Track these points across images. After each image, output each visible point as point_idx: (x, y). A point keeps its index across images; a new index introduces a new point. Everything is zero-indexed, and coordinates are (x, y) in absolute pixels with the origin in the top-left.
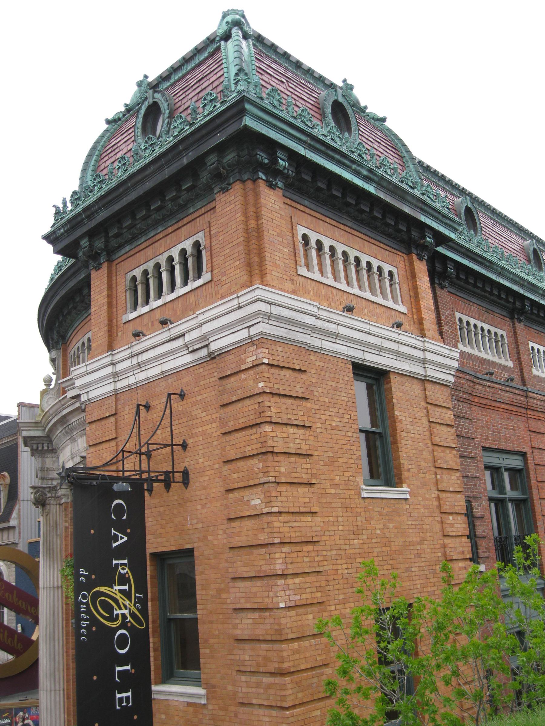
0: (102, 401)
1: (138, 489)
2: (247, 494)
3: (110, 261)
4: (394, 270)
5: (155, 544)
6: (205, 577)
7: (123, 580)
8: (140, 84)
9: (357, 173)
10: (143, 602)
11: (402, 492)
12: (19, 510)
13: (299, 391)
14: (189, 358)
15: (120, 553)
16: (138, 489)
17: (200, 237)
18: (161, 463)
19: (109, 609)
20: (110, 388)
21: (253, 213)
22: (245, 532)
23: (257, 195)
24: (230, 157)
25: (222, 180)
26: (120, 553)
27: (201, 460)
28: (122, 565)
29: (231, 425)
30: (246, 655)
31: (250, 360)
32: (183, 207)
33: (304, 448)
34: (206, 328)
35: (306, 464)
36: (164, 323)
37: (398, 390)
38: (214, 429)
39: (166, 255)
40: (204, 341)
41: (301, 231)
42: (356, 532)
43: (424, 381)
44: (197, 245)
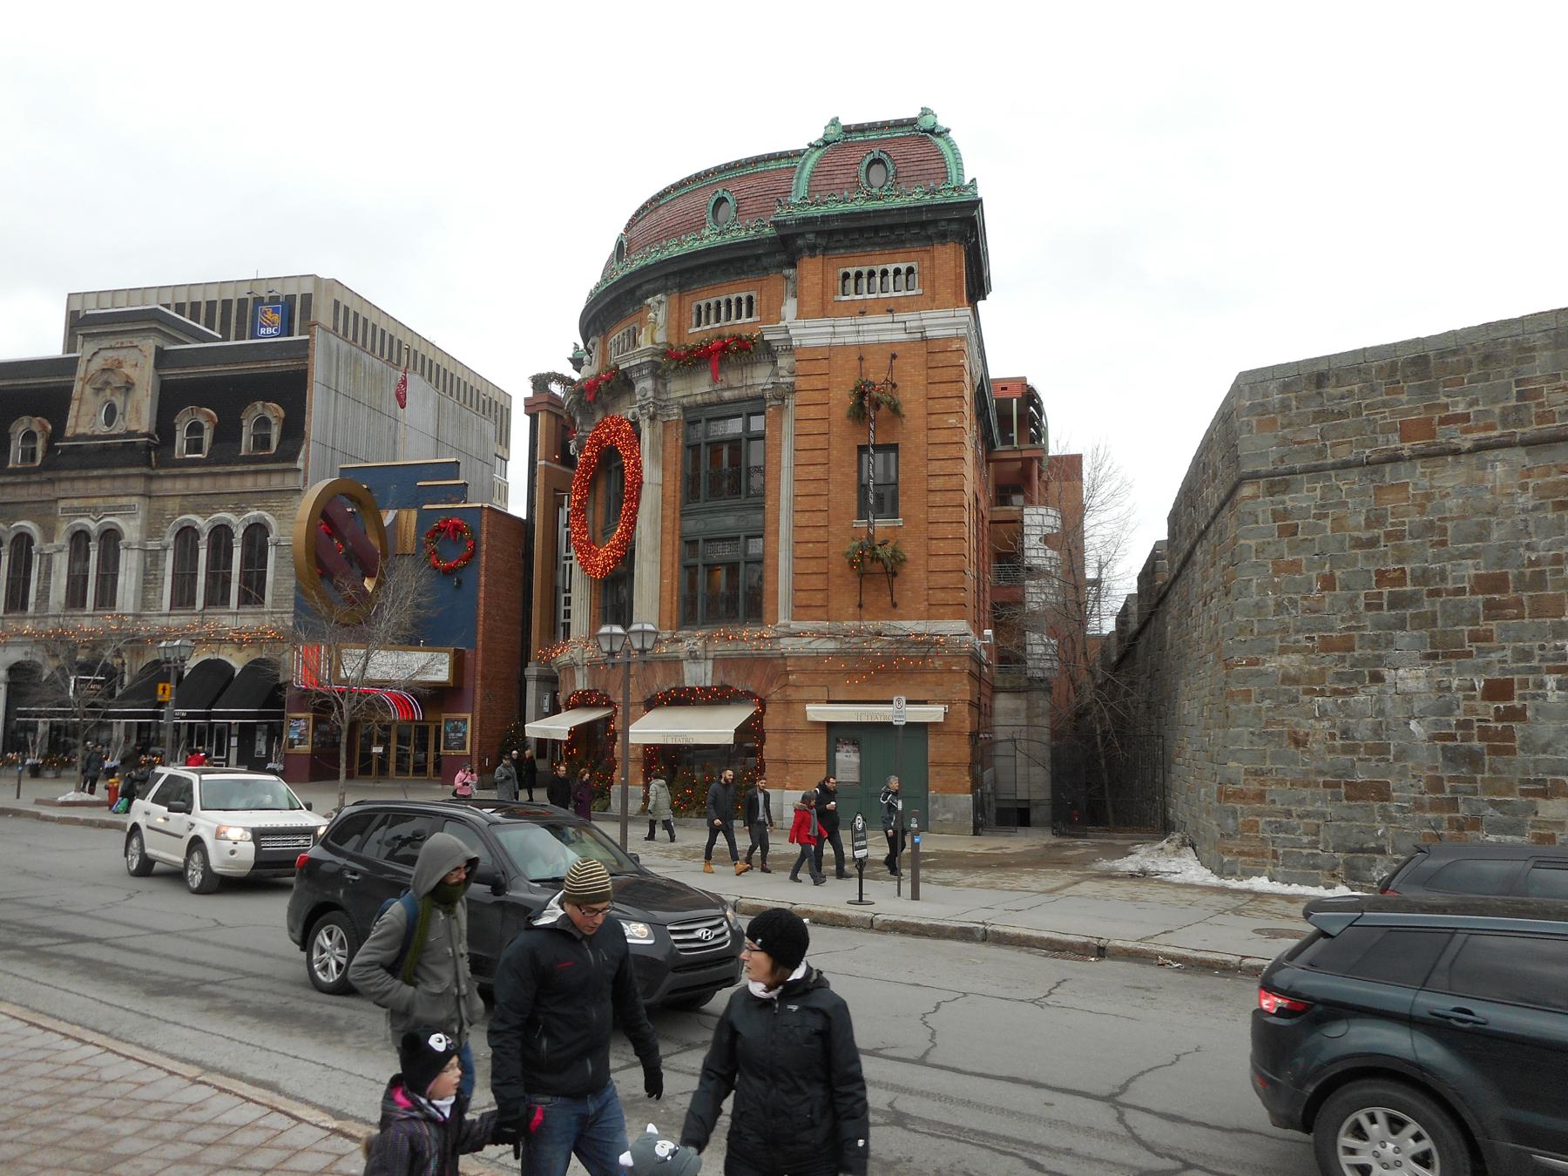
2: (945, 417)
12: (307, 452)
14: (905, 336)
17: (914, 265)
20: (825, 341)
22: (942, 436)
24: (954, 227)
25: (943, 237)
29: (937, 379)
30: (938, 499)
31: (954, 347)
32: (903, 242)
34: (925, 323)
36: (891, 311)
38: (921, 379)
39: (881, 267)
40: (923, 330)
44: (910, 271)
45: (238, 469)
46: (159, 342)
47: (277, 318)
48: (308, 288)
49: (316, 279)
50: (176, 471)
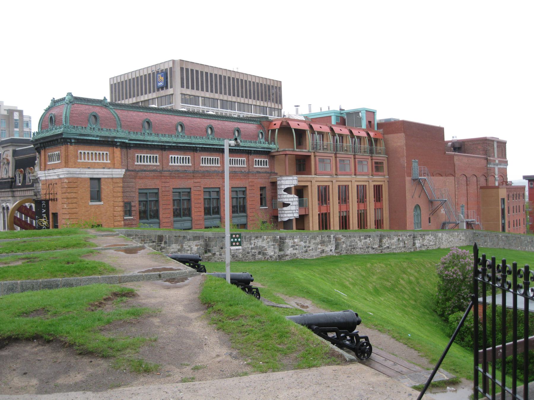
0: (43, 181)
1: (47, 202)
3: (45, 149)
4: (108, 153)
5: (51, 211)
6: (59, 218)
7: (45, 218)
8: (52, 100)
9: (94, 137)
10: (49, 222)
11: (102, 203)
13: (75, 186)
15: (44, 213)
16: (47, 202)
18: (51, 197)
19: (42, 223)
21: (67, 151)
23: (67, 147)
26: (44, 213)
27: (59, 196)
28: (44, 215)
33: (75, 197)
35: (76, 200)
37: (103, 182)
41: (79, 151)
42: (87, 211)
43: (112, 178)
45: (25, 189)
46: (14, 148)
47: (162, 79)
48: (171, 65)
49: (174, 61)
50: (19, 189)
